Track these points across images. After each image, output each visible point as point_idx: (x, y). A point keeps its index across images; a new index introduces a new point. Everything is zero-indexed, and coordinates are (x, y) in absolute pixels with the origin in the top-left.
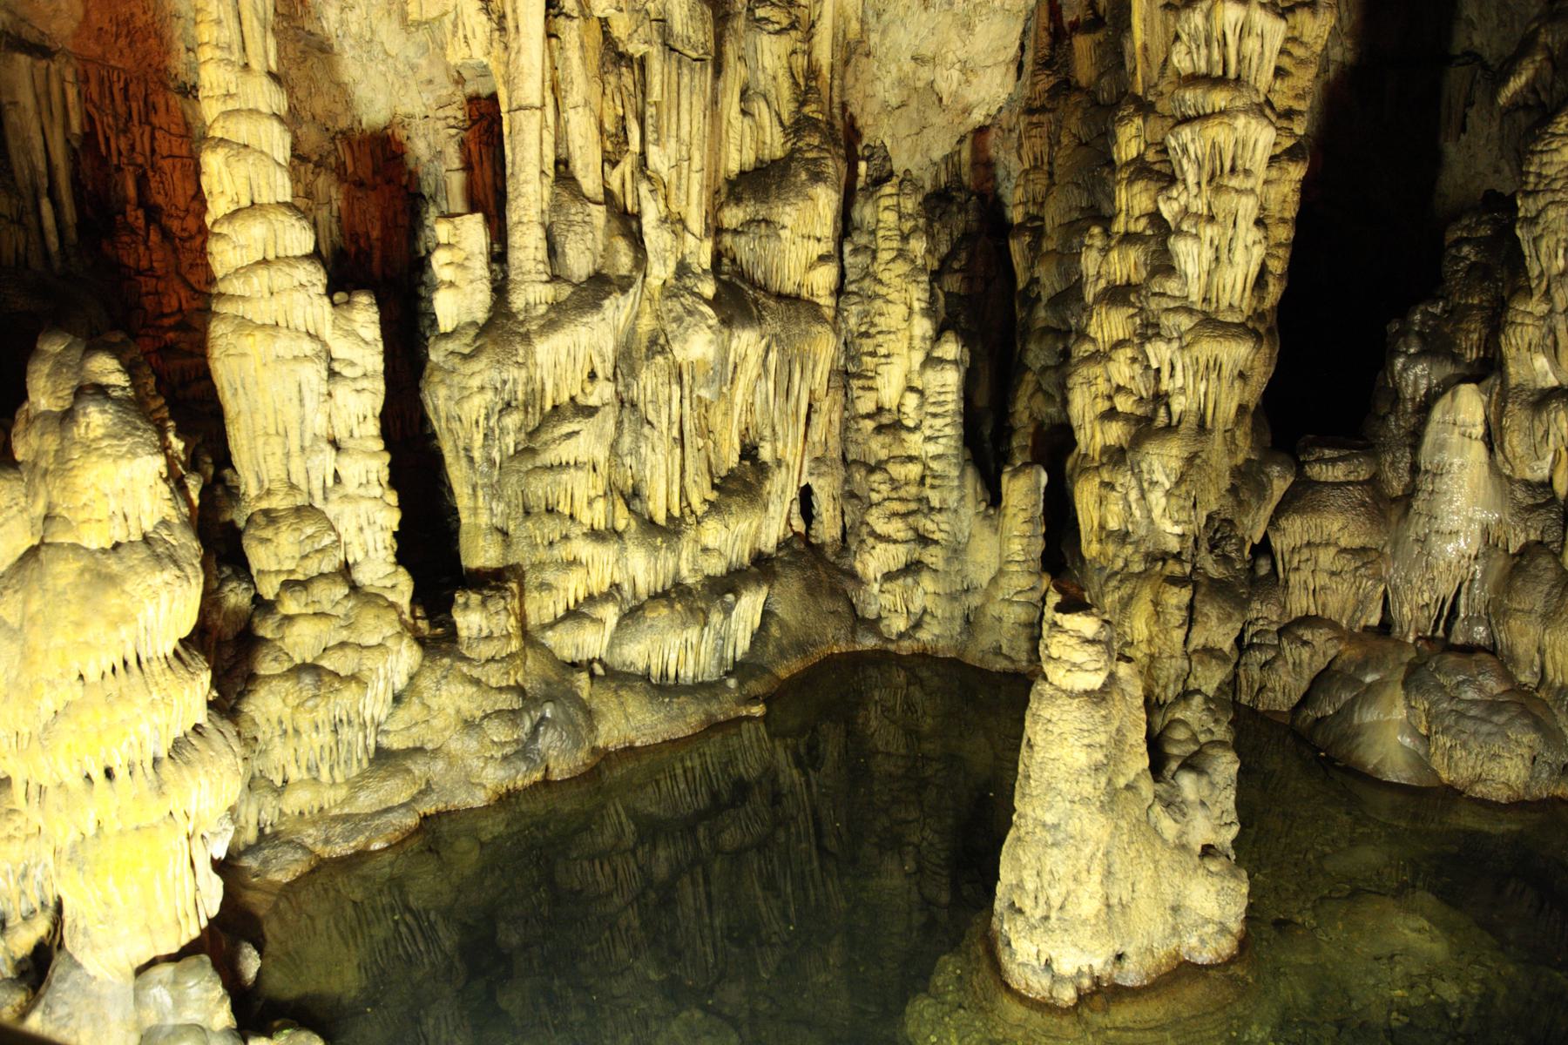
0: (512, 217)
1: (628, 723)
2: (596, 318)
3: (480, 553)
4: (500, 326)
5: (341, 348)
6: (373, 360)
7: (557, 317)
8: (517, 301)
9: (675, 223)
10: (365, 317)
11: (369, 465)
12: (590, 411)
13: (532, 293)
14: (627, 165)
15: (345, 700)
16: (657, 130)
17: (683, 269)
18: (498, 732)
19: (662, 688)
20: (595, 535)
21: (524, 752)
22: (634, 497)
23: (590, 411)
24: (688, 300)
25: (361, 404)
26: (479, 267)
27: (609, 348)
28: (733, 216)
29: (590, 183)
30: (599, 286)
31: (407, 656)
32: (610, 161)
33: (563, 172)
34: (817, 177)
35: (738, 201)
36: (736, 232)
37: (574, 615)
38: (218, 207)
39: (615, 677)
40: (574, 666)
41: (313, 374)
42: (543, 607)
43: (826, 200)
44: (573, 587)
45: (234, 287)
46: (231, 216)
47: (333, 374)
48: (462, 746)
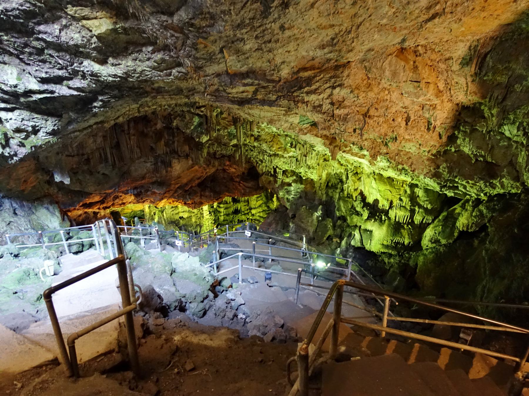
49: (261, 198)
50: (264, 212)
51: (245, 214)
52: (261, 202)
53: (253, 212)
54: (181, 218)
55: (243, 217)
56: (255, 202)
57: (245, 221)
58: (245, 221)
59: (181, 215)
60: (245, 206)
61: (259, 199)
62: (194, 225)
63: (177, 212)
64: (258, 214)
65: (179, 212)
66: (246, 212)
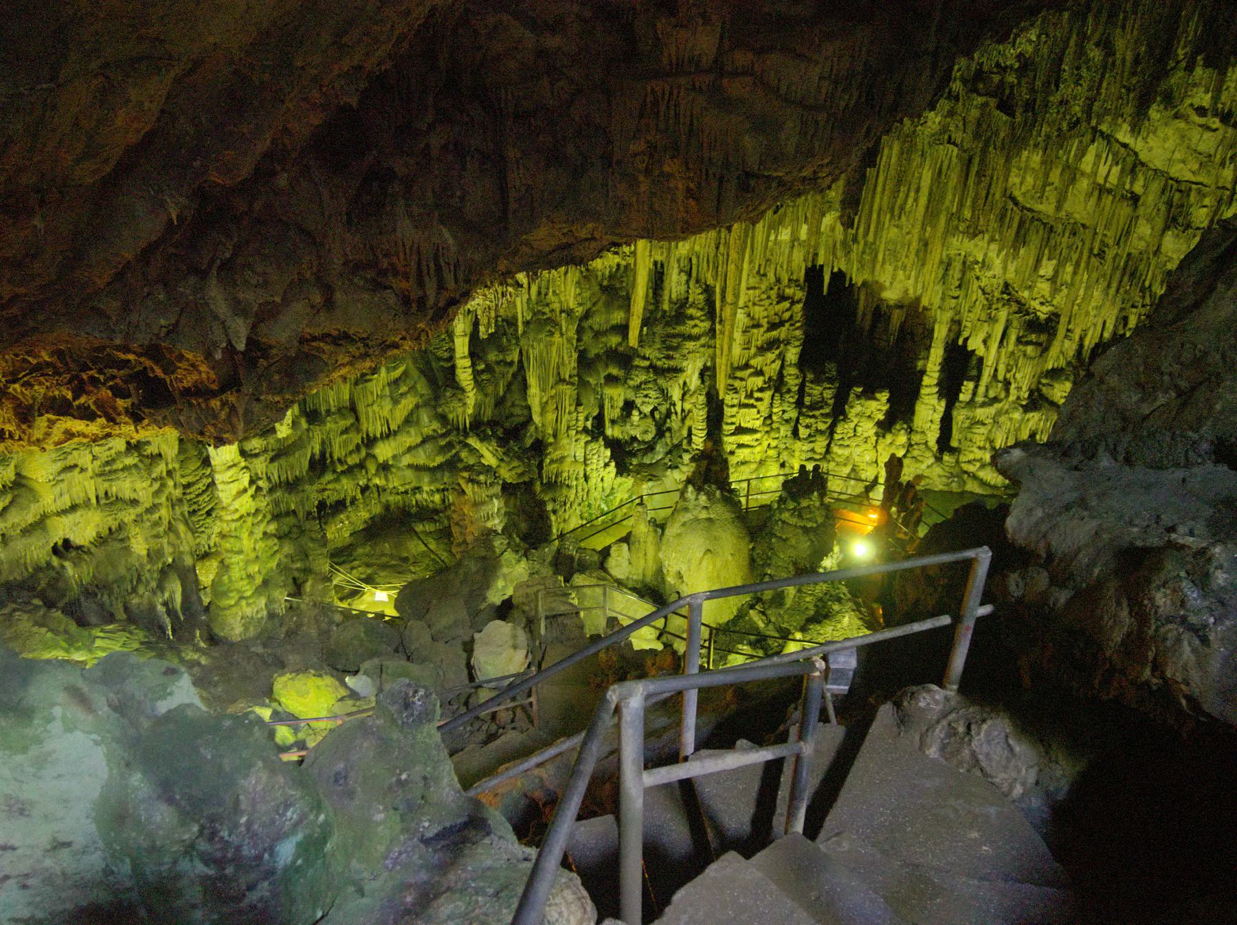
1: (972, 486)
3: (954, 444)
4: (971, 403)
6: (943, 410)
7: (983, 405)
9: (1019, 389)
10: (943, 403)
11: (936, 427)
12: (984, 424)
15: (919, 465)
17: (1018, 398)
18: (944, 480)
19: (983, 483)
20: (979, 448)
21: (947, 485)
22: (992, 442)
23: (984, 424)
25: (937, 417)
28: (1044, 381)
29: (1000, 377)
30: (996, 400)
31: (932, 460)
32: (1008, 371)
33: (995, 376)
34: (1067, 379)
35: (1046, 377)
37: (969, 462)
38: (924, 383)
39: (975, 477)
40: (966, 472)
42: (962, 458)
43: (1068, 386)
44: (971, 457)
48: (936, 479)
49: (410, 382)
50: (429, 447)
51: (350, 471)
52: (408, 403)
53: (384, 451)
54: (65, 548)
55: (347, 487)
56: (387, 404)
57: (354, 501)
58: (354, 501)
59: (61, 529)
60: (346, 431)
61: (403, 389)
62: (150, 573)
63: (30, 519)
64: (407, 460)
65: (44, 517)
66: (353, 460)
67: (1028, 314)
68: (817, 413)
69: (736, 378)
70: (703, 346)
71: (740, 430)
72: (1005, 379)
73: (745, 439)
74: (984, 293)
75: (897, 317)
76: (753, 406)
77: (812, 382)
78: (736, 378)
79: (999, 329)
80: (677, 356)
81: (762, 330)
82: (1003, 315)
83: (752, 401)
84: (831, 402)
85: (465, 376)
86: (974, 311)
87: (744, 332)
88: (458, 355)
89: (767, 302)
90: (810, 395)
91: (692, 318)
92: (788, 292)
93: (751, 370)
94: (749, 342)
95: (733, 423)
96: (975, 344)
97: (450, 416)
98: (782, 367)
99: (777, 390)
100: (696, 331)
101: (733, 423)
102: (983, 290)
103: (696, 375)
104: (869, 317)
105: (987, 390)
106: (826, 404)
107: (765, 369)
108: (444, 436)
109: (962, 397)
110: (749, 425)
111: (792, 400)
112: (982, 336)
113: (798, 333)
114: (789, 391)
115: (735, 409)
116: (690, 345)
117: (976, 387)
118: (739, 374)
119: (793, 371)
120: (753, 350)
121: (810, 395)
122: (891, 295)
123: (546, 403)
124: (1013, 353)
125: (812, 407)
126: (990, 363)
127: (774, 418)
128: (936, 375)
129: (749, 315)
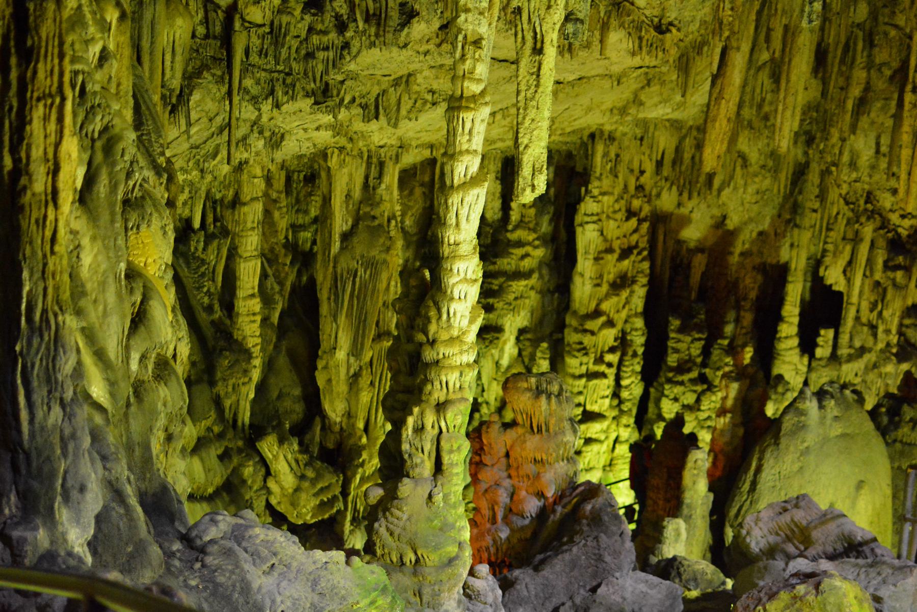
0: (841, 330)
2: (860, 360)
5: (800, 367)
6: (805, 369)
8: (839, 352)
9: (888, 332)
10: (806, 360)
13: (843, 351)
14: (875, 313)
16: (887, 305)
24: (888, 354)
26: (831, 343)
27: (863, 367)
28: (907, 321)
30: (862, 350)
32: (872, 311)
35: (909, 316)
36: (907, 327)
41: (794, 373)
45: (782, 353)
46: (786, 338)
47: (797, 373)
67: (889, 232)
68: (686, 377)
69: (585, 331)
70: (532, 288)
71: (589, 417)
72: (869, 321)
73: (594, 429)
74: (847, 203)
75: (699, 263)
76: (604, 375)
77: (681, 330)
78: (585, 331)
79: (864, 249)
80: (499, 305)
81: (616, 256)
82: (868, 231)
83: (603, 368)
84: (699, 360)
85: (250, 327)
86: (836, 227)
87: (597, 259)
88: (241, 294)
89: (619, 216)
90: (676, 351)
91: (520, 244)
92: (636, 203)
93: (603, 319)
94: (601, 276)
95: (579, 405)
96: (834, 277)
97: (227, 403)
98: (626, 321)
99: (624, 354)
100: (527, 264)
101: (579, 405)
102: (845, 199)
103: (512, 339)
104: (668, 266)
105: (851, 339)
106: (695, 364)
107: (616, 317)
108: (221, 436)
109: (819, 352)
110: (595, 408)
111: (638, 368)
112: (842, 262)
113: (646, 265)
114: (635, 355)
115: (584, 380)
116: (519, 286)
117: (836, 337)
118: (590, 325)
119: (639, 323)
120: (605, 288)
121: (676, 351)
122: (692, 234)
123: (356, 376)
124: (878, 284)
125: (682, 368)
126: (855, 299)
127: (625, 394)
128: (796, 320)
129: (602, 234)
